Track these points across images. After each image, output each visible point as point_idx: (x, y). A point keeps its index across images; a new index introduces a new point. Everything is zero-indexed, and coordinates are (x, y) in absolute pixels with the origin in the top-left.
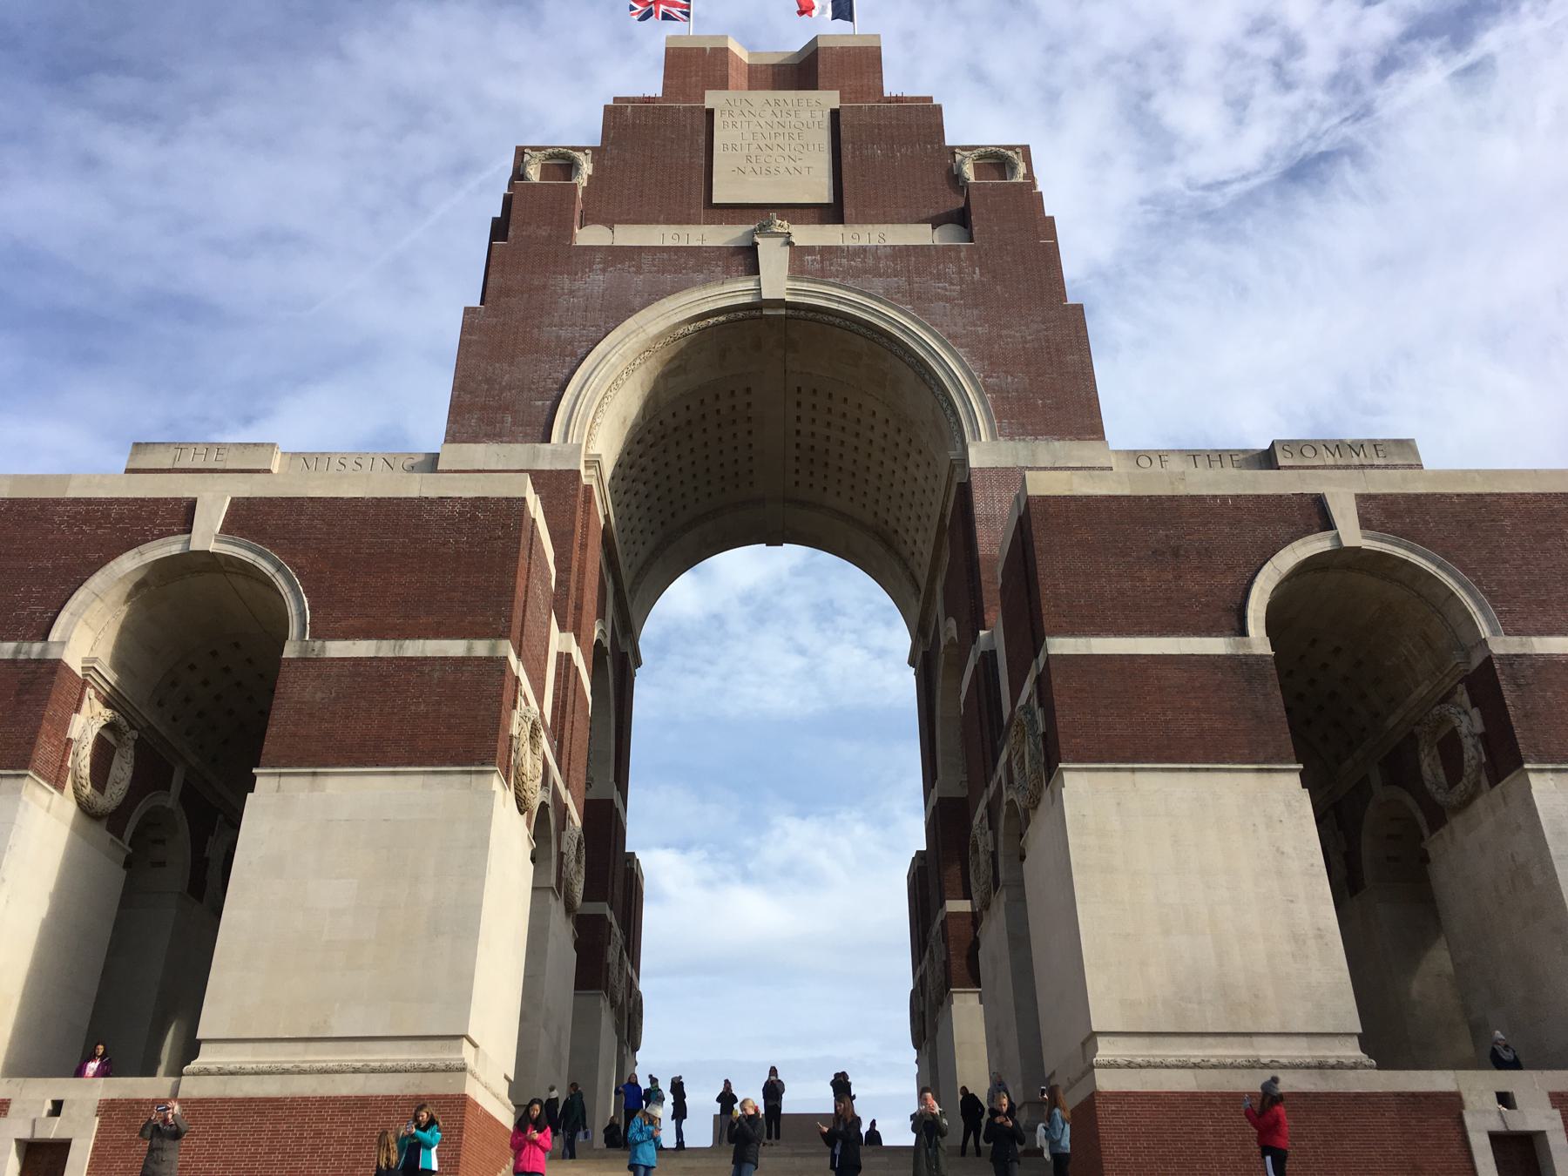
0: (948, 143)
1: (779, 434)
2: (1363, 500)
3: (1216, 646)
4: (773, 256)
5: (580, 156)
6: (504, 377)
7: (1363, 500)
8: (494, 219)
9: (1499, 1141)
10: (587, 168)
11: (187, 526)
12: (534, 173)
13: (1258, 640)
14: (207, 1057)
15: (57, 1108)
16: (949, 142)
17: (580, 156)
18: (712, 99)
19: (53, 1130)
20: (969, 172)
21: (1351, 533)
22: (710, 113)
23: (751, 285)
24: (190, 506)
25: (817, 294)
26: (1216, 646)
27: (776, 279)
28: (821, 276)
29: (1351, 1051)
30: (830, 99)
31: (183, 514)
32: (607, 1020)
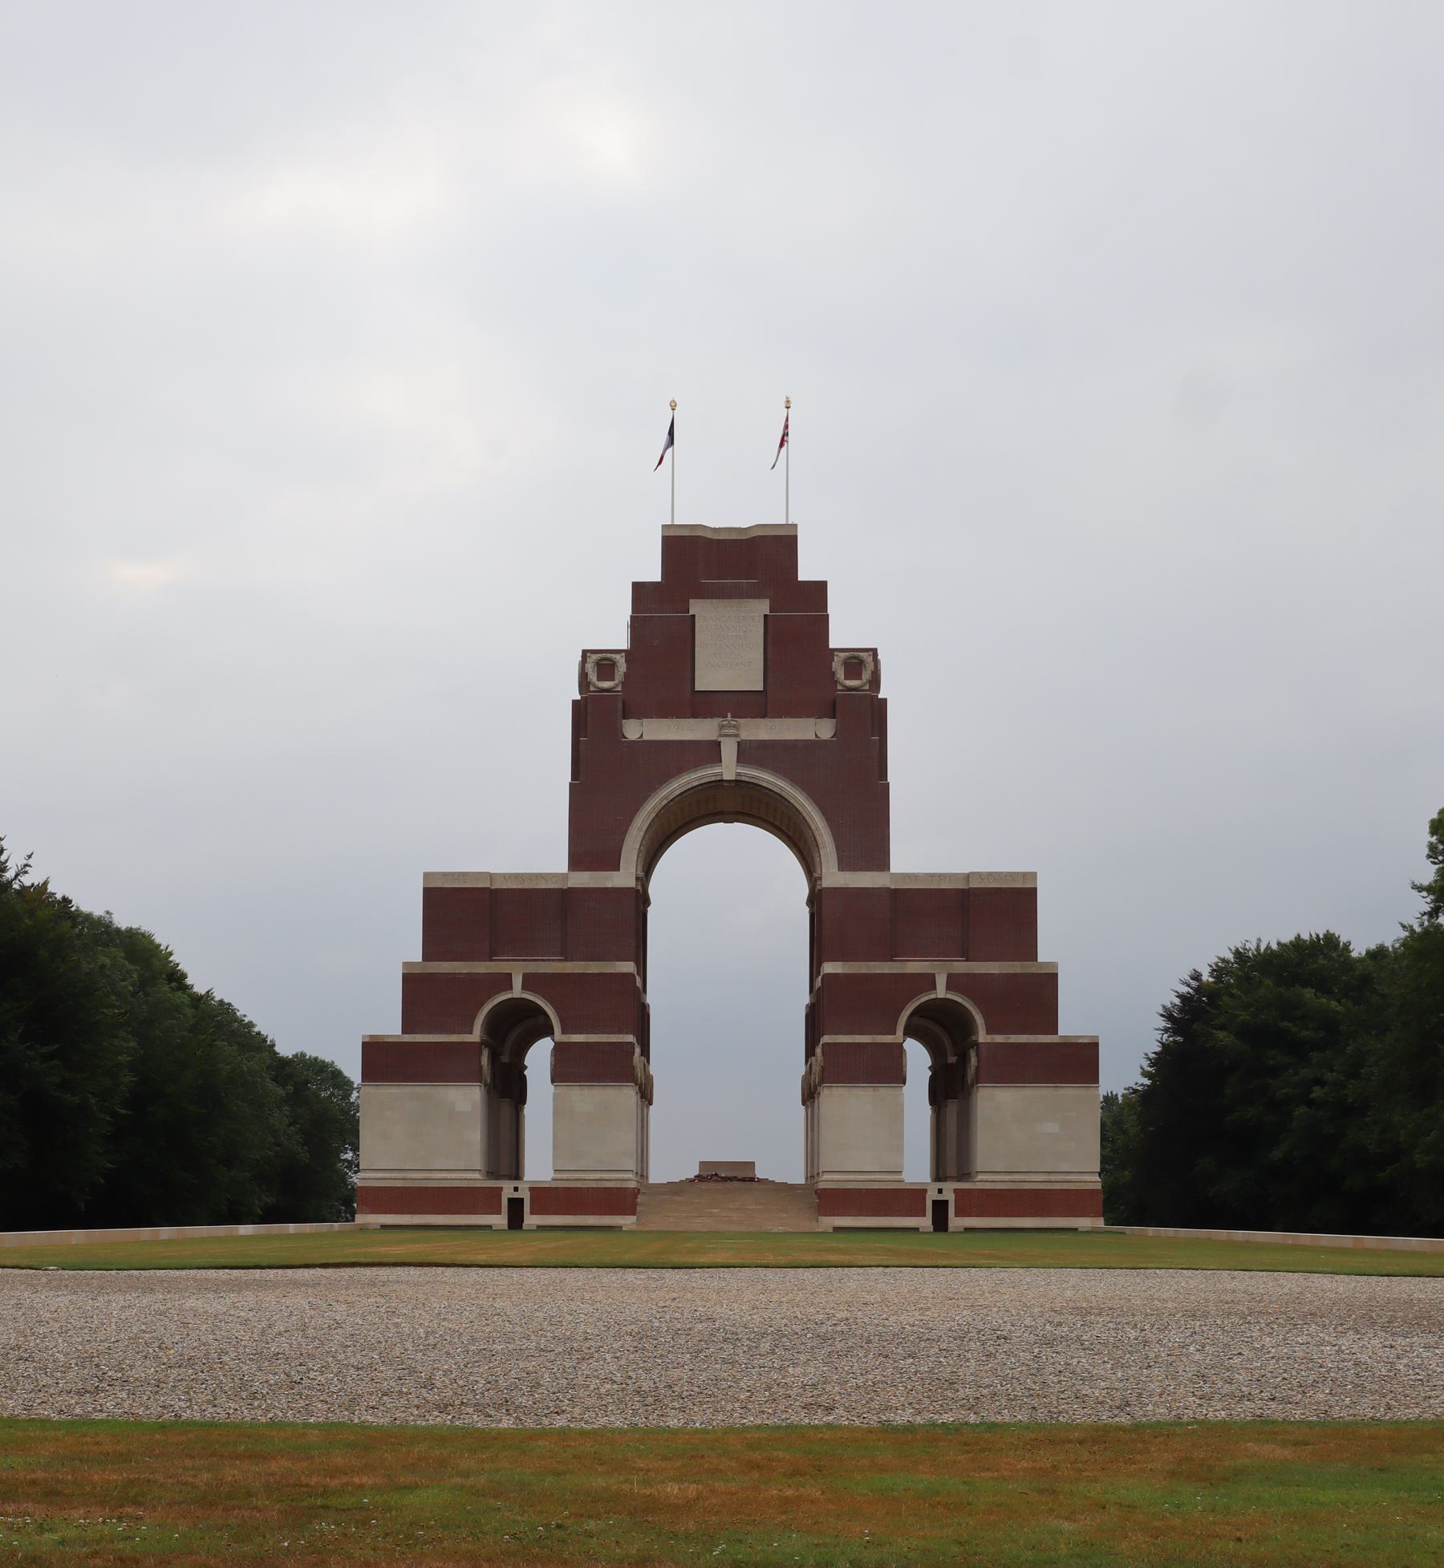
0: (832, 645)
4: (729, 751)
5: (617, 657)
8: (574, 702)
9: (934, 1202)
11: (510, 987)
12: (593, 677)
16: (832, 645)
17: (617, 657)
18: (696, 607)
19: (516, 1195)
20: (840, 674)
21: (941, 992)
23: (717, 770)
27: (729, 768)
30: (763, 607)
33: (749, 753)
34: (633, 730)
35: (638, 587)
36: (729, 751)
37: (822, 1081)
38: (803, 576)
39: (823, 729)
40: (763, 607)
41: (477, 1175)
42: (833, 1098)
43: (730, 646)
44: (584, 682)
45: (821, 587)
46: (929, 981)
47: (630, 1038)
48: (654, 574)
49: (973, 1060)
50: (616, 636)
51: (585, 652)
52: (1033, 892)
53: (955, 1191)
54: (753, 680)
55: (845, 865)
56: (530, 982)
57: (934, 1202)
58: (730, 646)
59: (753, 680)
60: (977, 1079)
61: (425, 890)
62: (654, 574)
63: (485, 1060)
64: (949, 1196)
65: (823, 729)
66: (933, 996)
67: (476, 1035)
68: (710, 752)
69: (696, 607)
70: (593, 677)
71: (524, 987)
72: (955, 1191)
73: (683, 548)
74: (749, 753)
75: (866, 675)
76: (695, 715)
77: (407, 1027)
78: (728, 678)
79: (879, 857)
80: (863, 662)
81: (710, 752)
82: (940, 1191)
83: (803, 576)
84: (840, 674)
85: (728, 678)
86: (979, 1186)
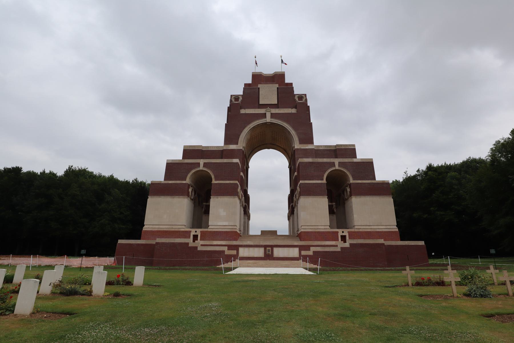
0: (295, 93)
1: (269, 137)
2: (339, 163)
3: (320, 182)
4: (268, 115)
6: (231, 135)
7: (339, 163)
9: (341, 236)
10: (241, 98)
11: (199, 166)
13: (324, 181)
14: (210, 227)
15: (196, 232)
16: (295, 93)
18: (259, 86)
19: (196, 234)
20: (297, 99)
21: (337, 167)
22: (259, 88)
24: (199, 163)
25: (275, 121)
26: (320, 182)
27: (268, 119)
28: (276, 118)
29: (328, 227)
30: (277, 86)
31: (198, 164)
32: (246, 218)
33: (273, 116)
34: (243, 111)
35: (246, 85)
36: (268, 115)
37: (301, 194)
38: (287, 81)
39: (294, 111)
40: (277, 86)
41: (183, 227)
42: (304, 202)
43: (268, 94)
44: (231, 101)
45: (291, 84)
46: (333, 164)
47: (237, 182)
48: (250, 81)
49: (348, 190)
50: (240, 92)
51: (231, 96)
52: (355, 149)
53: (348, 232)
54: (275, 102)
55: (300, 143)
56: (205, 165)
57: (341, 236)
58: (268, 94)
59: (275, 102)
60: (351, 195)
61: (184, 150)
62: (250, 81)
63: (190, 190)
64: (346, 233)
65: (294, 111)
66: (333, 169)
67: (188, 181)
68: (264, 116)
69: (259, 86)
70: (233, 100)
71: (204, 166)
72: (348, 232)
73: (258, 78)
74: (273, 116)
75: (304, 100)
76: (259, 108)
77: (165, 180)
78: (268, 112)
79: (310, 141)
80: (302, 97)
81: (264, 116)
82: (343, 232)
83: (287, 81)
84: (297, 99)
85: (268, 112)
86: (356, 230)
